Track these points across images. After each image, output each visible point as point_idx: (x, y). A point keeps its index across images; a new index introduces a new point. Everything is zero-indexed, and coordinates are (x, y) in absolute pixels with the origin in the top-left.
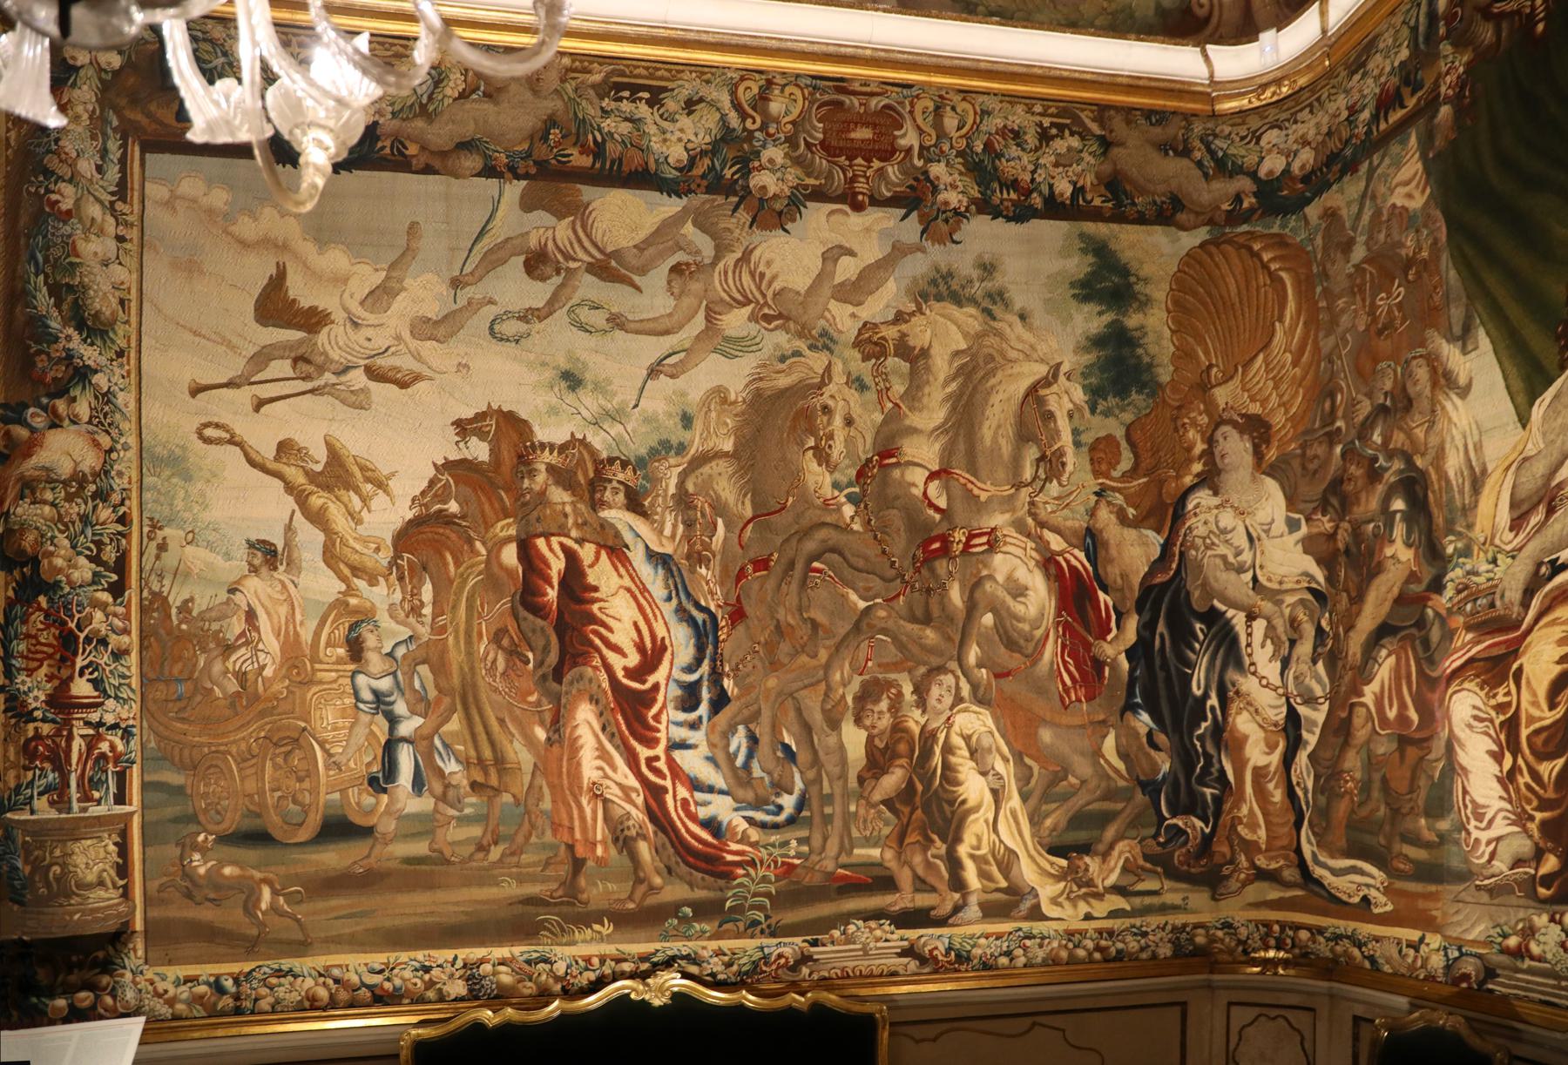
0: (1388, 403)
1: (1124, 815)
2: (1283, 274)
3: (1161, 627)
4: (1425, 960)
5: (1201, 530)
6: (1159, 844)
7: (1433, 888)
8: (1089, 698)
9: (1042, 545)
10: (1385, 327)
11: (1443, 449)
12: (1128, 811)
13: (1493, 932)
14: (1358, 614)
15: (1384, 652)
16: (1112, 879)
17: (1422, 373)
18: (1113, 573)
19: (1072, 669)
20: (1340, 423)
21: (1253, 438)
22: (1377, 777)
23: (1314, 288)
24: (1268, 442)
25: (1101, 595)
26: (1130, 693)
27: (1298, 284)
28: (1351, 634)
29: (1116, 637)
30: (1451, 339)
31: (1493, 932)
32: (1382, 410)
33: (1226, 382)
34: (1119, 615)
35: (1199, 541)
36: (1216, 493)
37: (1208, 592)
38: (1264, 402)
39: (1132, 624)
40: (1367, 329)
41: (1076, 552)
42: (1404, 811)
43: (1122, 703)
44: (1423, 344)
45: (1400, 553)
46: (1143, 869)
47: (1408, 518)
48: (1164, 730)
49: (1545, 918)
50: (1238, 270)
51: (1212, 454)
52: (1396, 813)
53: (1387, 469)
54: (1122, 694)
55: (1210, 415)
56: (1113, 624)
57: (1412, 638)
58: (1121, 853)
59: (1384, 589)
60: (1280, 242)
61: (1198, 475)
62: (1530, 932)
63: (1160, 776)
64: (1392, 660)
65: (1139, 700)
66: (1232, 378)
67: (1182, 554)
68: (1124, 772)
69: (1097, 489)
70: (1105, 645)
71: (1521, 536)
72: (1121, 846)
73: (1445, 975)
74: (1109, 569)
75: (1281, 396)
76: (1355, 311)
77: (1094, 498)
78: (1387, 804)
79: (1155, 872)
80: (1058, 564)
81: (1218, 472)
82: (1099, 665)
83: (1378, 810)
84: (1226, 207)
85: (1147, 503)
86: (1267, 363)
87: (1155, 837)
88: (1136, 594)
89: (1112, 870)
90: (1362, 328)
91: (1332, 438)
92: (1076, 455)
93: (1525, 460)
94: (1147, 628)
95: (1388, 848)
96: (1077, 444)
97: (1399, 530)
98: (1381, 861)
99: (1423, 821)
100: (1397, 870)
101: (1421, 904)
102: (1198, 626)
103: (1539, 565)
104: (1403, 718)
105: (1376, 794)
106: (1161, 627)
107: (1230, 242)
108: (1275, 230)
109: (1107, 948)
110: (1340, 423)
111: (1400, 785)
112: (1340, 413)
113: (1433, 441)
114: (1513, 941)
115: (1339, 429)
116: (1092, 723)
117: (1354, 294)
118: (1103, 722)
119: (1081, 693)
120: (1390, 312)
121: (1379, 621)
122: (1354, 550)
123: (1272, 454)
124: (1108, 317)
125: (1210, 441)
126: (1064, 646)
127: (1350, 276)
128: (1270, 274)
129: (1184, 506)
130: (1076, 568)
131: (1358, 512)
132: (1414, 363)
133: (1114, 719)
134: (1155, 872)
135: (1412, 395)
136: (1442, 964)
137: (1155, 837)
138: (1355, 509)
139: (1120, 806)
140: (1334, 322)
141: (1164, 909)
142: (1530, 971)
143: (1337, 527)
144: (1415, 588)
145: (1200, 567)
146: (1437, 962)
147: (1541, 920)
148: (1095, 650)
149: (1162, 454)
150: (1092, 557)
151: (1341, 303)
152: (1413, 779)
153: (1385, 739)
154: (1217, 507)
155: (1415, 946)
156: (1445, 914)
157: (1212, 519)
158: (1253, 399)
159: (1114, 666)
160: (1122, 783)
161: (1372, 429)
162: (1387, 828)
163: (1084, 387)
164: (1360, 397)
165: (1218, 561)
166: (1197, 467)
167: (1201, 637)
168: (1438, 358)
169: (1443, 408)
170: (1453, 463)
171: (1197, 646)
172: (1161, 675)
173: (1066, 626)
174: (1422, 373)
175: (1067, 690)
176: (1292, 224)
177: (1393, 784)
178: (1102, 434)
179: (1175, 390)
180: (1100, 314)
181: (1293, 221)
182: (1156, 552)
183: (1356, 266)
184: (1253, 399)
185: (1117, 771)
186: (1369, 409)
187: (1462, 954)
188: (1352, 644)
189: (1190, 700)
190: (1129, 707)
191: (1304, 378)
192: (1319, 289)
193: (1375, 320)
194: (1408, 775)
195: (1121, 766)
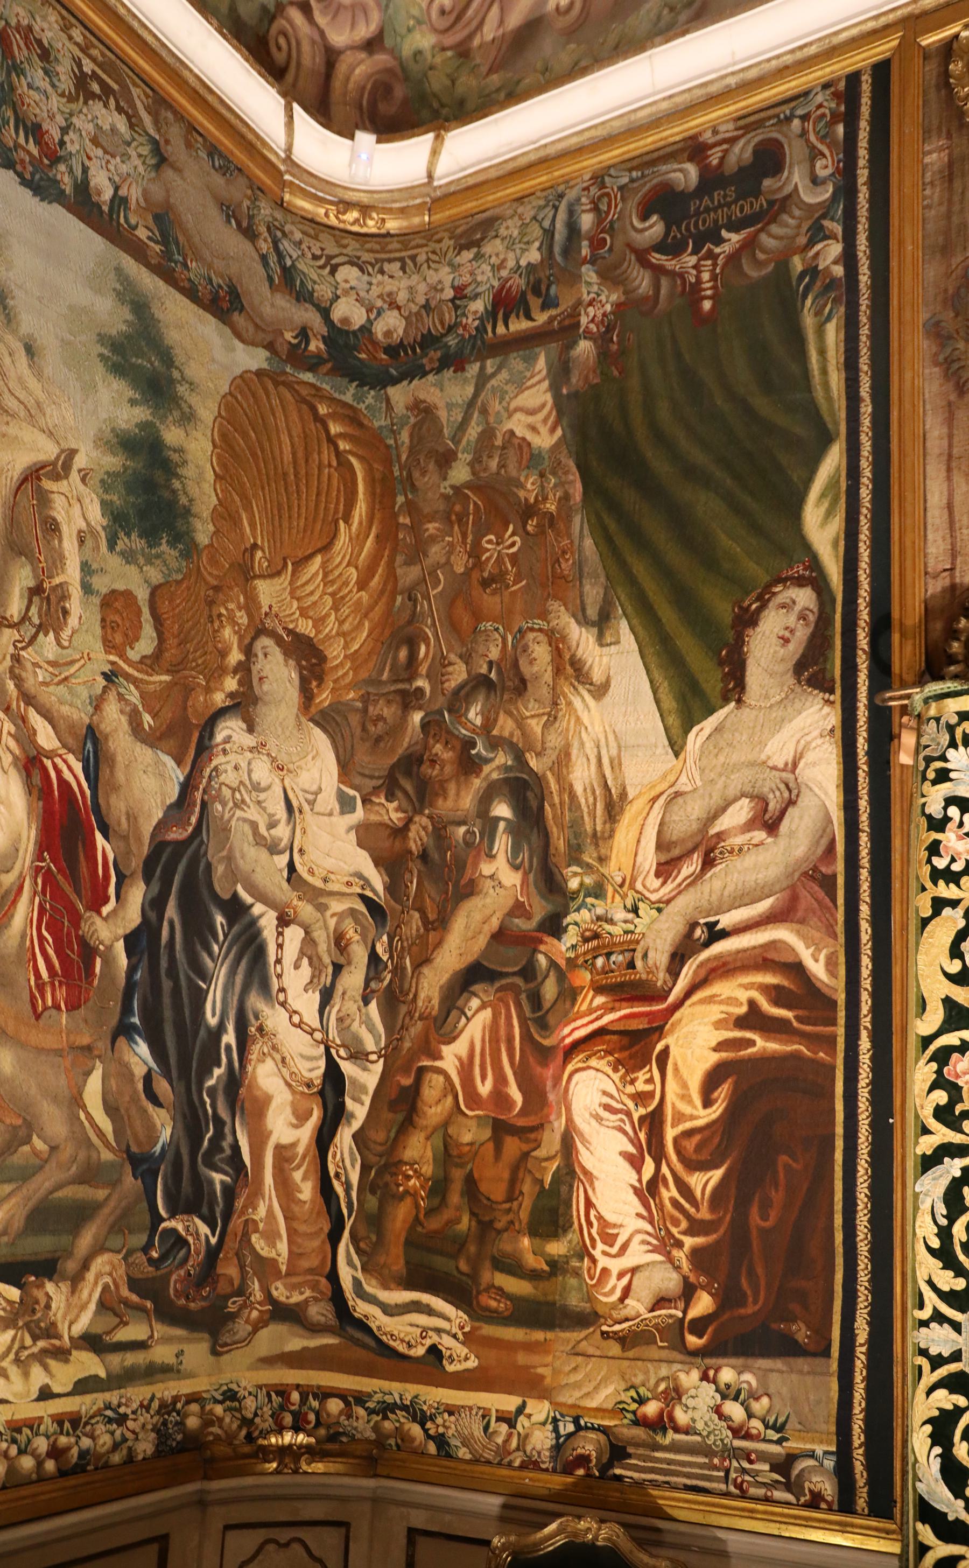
0: (493, 675)
1: (106, 1211)
2: (353, 460)
3: (171, 911)
4: (524, 1439)
5: (229, 777)
6: (151, 1261)
7: (539, 1335)
8: (73, 1006)
9: (26, 736)
10: (492, 580)
11: (568, 755)
12: (112, 1203)
13: (625, 1397)
14: (439, 944)
16: (83, 1323)
17: (541, 652)
18: (117, 807)
19: (51, 952)
20: (420, 683)
21: (301, 668)
22: (458, 1175)
23: (394, 496)
24: (321, 680)
25: (99, 837)
26: (127, 1010)
27: (371, 481)
28: (426, 970)
29: (114, 912)
30: (583, 621)
31: (625, 1397)
32: (480, 683)
33: (271, 576)
34: (121, 878)
35: (226, 792)
36: (251, 730)
37: (234, 875)
38: (319, 622)
39: (137, 894)
40: (468, 573)
41: (71, 758)
42: (499, 1225)
43: (114, 1021)
44: (544, 615)
46: (126, 1303)
48: (167, 1075)
49: (695, 1374)
50: (297, 430)
51: (249, 671)
52: (485, 1228)
53: (488, 761)
54: (115, 1006)
55: (250, 616)
56: (112, 890)
57: (513, 988)
58: (99, 1276)
59: (478, 917)
60: (352, 417)
61: (231, 695)
62: (674, 1394)
63: (158, 1148)
65: (136, 1020)
66: (278, 573)
67: (204, 804)
68: (111, 1137)
69: (107, 668)
70: (98, 921)
71: (670, 886)
72: (100, 1263)
73: (554, 1458)
74: (113, 800)
75: (341, 623)
76: (451, 544)
77: (102, 682)
78: (472, 1214)
79: (143, 1310)
80: (44, 769)
81: (255, 700)
82: (88, 952)
83: (458, 1221)
84: (289, 336)
85: (167, 714)
86: (324, 565)
87: (146, 1249)
88: (145, 850)
89: (83, 1307)
90: (460, 569)
91: (409, 700)
92: (85, 604)
93: (678, 794)
94: (155, 905)
95: (474, 1276)
96: (87, 588)
97: (502, 843)
99: (526, 1242)
100: (488, 1309)
101: (522, 1358)
102: (219, 919)
103: (693, 925)
104: (500, 1097)
105: (455, 1198)
106: (171, 911)
107: (289, 385)
108: (348, 398)
109: (68, 1449)
110: (420, 683)
111: (495, 1189)
112: (423, 669)
113: (554, 740)
114: (652, 1409)
115: (420, 690)
116: (72, 1048)
117: (451, 524)
118: (88, 1048)
119: (61, 994)
120: (500, 560)
121: (469, 959)
122: (435, 856)
123: (324, 698)
124: (141, 414)
125: (248, 651)
126: (42, 910)
127: (446, 497)
128: (338, 453)
129: (212, 735)
130: (68, 784)
131: (444, 807)
132: (531, 635)
133: (102, 1046)
134: (143, 1310)
135: (527, 676)
136: (549, 1443)
137: (146, 1249)
138: (440, 802)
139: (101, 1194)
140: (417, 553)
141: (153, 1372)
142: (675, 1448)
143: (410, 821)
144: (521, 924)
145: (226, 830)
146: (542, 1440)
147: (690, 1378)
148: (85, 928)
149: (190, 647)
150: (92, 774)
151: (432, 527)
152: (513, 1182)
153: (473, 1124)
154: (251, 750)
155: (510, 1420)
156: (556, 1372)
157: (244, 765)
158: (304, 612)
159: (109, 962)
160: (107, 1155)
161: (468, 703)
162: (472, 1249)
163: (103, 503)
164: (453, 657)
165: (247, 828)
166: (231, 684)
167: (221, 937)
168: (564, 638)
169: (569, 704)
171: (216, 948)
172: (167, 985)
173: (49, 878)
174: (541, 652)
175: (41, 987)
176: (369, 400)
177: (484, 1187)
178: (120, 586)
179: (213, 562)
180: (133, 402)
181: (371, 397)
182: (173, 793)
183: (457, 489)
184: (304, 612)
185: (100, 1134)
186: (464, 676)
187: (579, 1428)
188: (425, 983)
189: (202, 1033)
190: (123, 1030)
191: (371, 608)
192: (400, 499)
193: (479, 565)
194: (506, 1175)
195: (106, 1124)
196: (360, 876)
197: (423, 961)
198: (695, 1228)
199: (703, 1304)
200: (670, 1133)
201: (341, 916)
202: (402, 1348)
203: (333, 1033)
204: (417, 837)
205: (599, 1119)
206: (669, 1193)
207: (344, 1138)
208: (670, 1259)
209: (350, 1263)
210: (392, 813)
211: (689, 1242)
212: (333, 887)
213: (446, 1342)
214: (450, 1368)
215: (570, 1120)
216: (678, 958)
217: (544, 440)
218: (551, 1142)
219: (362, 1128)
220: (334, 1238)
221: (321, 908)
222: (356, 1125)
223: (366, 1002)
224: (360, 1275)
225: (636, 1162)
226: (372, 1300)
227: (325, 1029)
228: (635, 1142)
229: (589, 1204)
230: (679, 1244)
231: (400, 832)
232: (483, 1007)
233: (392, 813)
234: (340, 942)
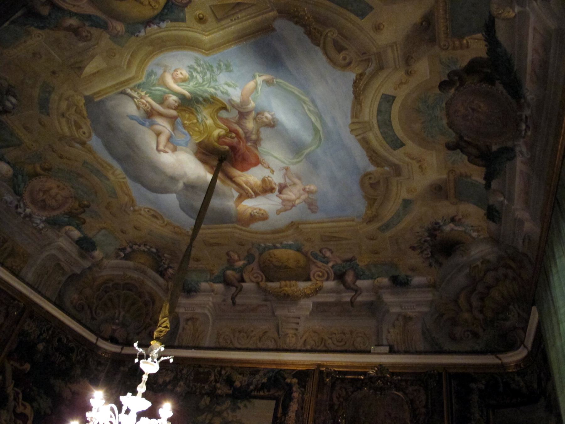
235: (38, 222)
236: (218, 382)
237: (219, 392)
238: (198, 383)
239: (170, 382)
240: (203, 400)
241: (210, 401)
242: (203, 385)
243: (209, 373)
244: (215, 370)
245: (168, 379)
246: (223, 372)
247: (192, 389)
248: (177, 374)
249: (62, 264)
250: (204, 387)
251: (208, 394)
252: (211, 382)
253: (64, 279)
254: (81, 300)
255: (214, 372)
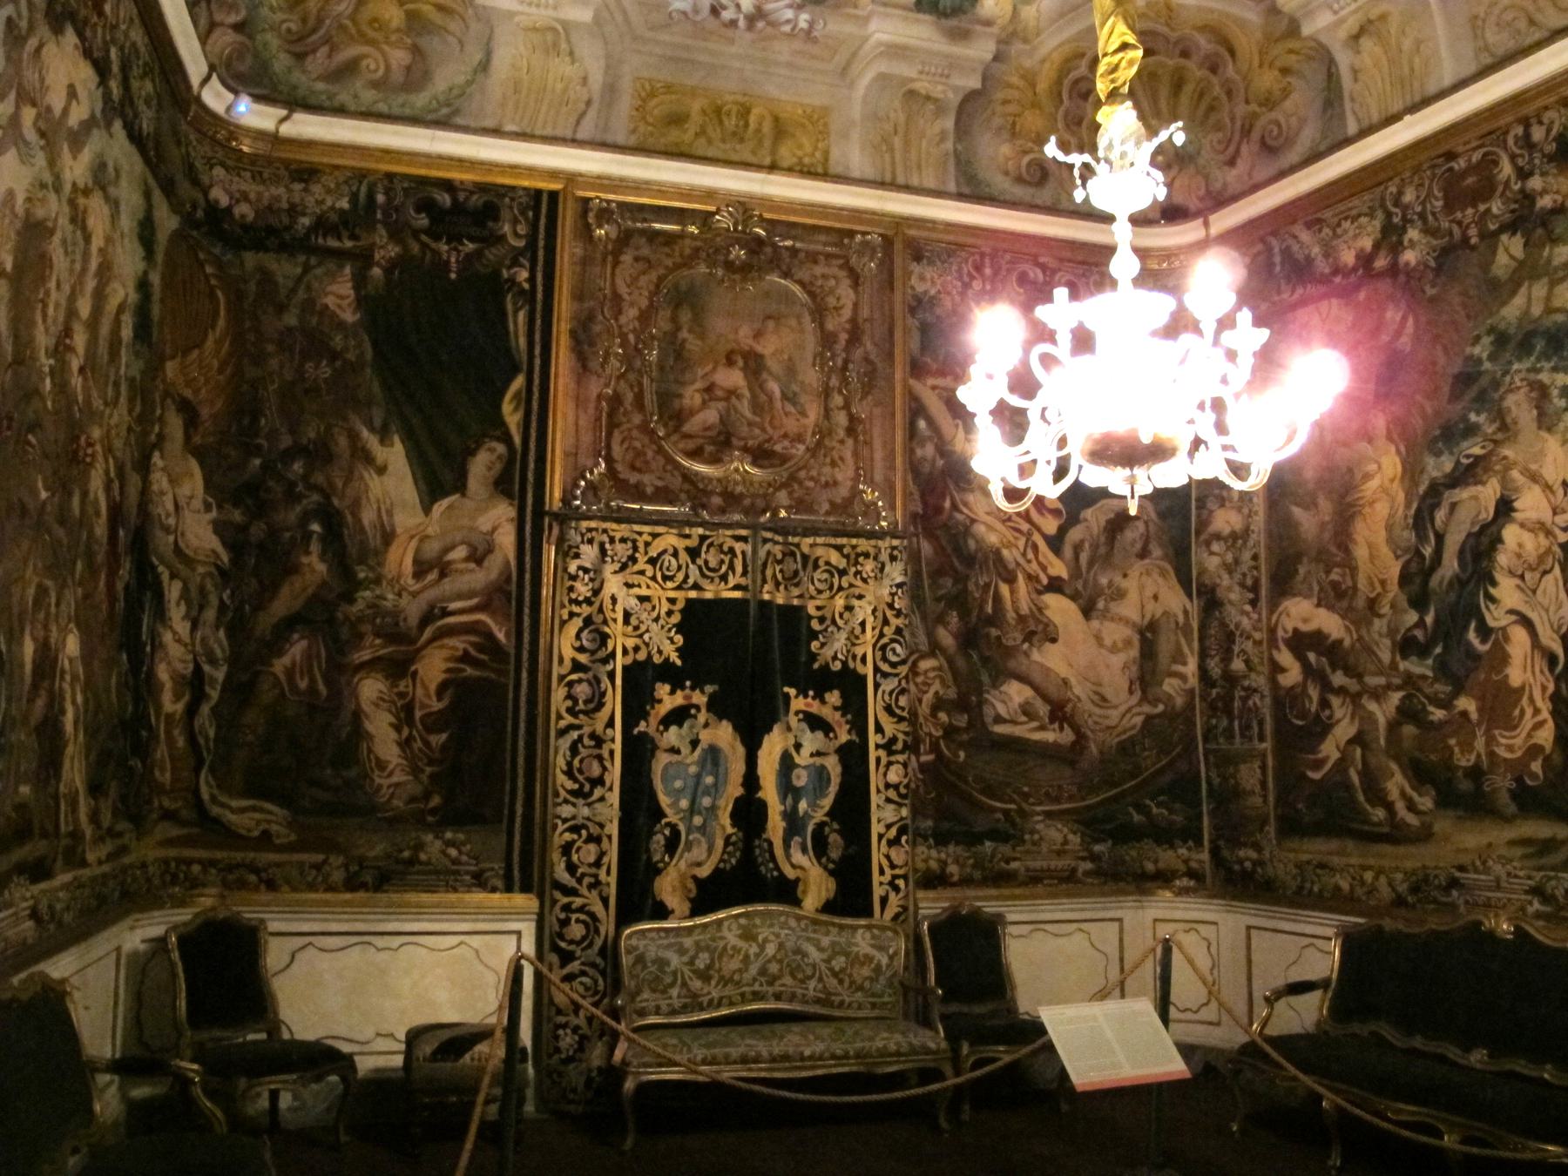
14: (271, 600)
15: (296, 636)
45: (315, 565)
47: (323, 539)
64: (304, 643)
91: (252, 450)
97: (315, 547)
98: (285, 800)
170: (368, 517)
196: (214, 551)
197: (259, 607)
198: (431, 762)
199: (436, 801)
200: (418, 714)
201: (204, 576)
202: (243, 832)
203: (198, 648)
204: (258, 531)
205: (377, 705)
206: (418, 744)
207: (205, 709)
208: (416, 777)
209: (207, 783)
210: (237, 516)
211: (428, 770)
212: (201, 558)
213: (274, 828)
214: (278, 842)
215: (358, 705)
216: (426, 620)
217: (349, 317)
218: (346, 716)
219: (216, 706)
220: (197, 771)
221: (194, 570)
222: (213, 702)
223: (217, 628)
224: (216, 791)
225: (398, 729)
226: (223, 805)
227: (193, 644)
228: (397, 717)
229: (370, 751)
230: (423, 771)
231: (243, 529)
232: (302, 638)
233: (237, 516)
234: (202, 591)
235: (789, 14)
236: (1531, 174)
237: (1545, 202)
238: (1463, 210)
239: (1377, 246)
240: (1501, 250)
241: (1526, 245)
242: (1482, 207)
243: (1490, 162)
244: (1505, 141)
245: (1367, 243)
246: (1538, 134)
247: (1451, 233)
248: (1389, 215)
249: (917, 86)
250: (1488, 210)
251: (1511, 227)
252: (1507, 183)
253: (949, 123)
254: (1025, 152)
255: (1506, 148)
